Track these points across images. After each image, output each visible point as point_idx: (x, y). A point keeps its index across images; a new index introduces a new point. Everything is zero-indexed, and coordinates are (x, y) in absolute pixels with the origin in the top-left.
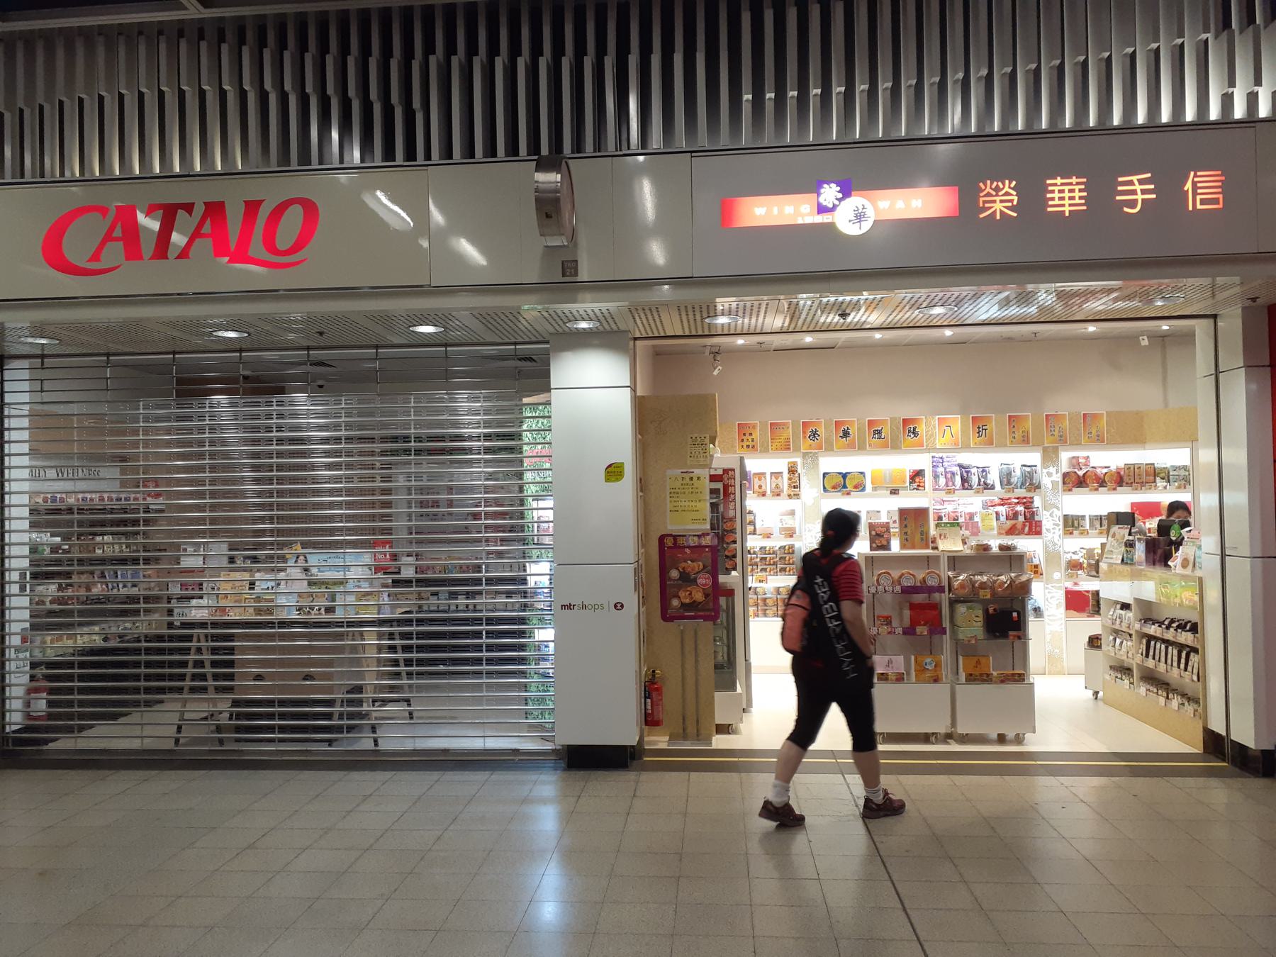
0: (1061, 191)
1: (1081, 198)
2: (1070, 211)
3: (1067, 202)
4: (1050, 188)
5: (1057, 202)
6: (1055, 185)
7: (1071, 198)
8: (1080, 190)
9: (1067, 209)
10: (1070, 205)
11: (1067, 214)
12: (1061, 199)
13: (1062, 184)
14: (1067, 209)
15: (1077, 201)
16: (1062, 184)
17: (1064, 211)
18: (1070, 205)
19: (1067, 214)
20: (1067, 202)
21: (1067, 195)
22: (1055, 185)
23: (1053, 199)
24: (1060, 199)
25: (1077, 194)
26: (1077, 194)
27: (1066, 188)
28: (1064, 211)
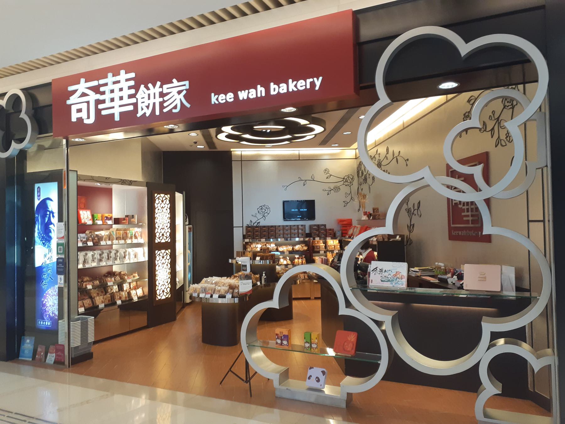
1: (130, 96)
2: (121, 114)
6: (106, 84)
8: (130, 88)
10: (120, 106)
11: (117, 118)
12: (112, 100)
15: (126, 101)
17: (113, 115)
18: (120, 106)
19: (117, 118)
20: (117, 102)
21: (116, 95)
22: (106, 84)
26: (126, 92)
27: (116, 87)
28: (113, 115)
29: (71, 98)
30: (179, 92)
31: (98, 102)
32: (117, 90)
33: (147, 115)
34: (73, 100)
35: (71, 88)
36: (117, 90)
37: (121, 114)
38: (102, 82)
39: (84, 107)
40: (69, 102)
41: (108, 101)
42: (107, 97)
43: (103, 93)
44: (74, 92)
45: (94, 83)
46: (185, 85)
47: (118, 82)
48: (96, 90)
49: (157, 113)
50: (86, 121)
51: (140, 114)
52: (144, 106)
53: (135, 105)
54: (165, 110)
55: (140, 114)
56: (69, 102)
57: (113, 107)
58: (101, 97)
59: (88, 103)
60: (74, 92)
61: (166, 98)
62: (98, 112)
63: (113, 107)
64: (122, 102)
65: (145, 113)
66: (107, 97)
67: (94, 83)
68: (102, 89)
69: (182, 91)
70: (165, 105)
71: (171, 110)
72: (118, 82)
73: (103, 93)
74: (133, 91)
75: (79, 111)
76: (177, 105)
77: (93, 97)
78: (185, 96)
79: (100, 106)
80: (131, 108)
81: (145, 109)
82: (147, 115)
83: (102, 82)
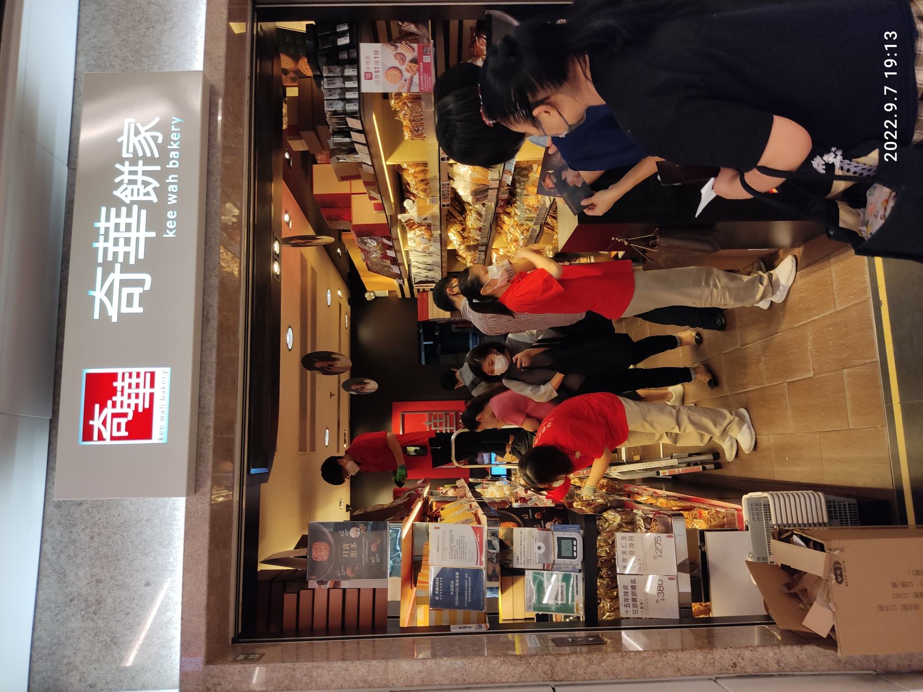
0: (116, 242)
1: (129, 214)
2: (148, 229)
3: (133, 235)
4: (110, 258)
5: (132, 249)
6: (106, 250)
7: (128, 227)
8: (118, 215)
9: (144, 234)
10: (138, 230)
11: (153, 234)
12: (127, 241)
13: (106, 240)
14: (144, 234)
15: (133, 220)
16: (106, 240)
18: (138, 230)
19: (153, 234)
20: (133, 235)
21: (122, 235)
22: (106, 250)
23: (127, 255)
24: (127, 241)
25: (123, 220)
26: (123, 220)
27: (112, 234)
29: (110, 315)
30: (137, 132)
31: (126, 268)
32: (117, 235)
33: (158, 185)
34: (113, 312)
35: (96, 316)
36: (117, 235)
37: (148, 229)
38: (100, 260)
39: (126, 291)
40: (114, 319)
41: (127, 249)
42: (121, 249)
43: (115, 254)
44: (102, 304)
45: (99, 270)
46: (129, 124)
47: (107, 229)
48: (108, 268)
49: (158, 168)
50: (147, 287)
51: (154, 198)
52: (143, 191)
53: (142, 205)
54: (157, 155)
55: (154, 198)
56: (114, 319)
57: (138, 239)
58: (121, 259)
59: (124, 283)
60: (102, 305)
61: (141, 154)
62: (140, 266)
63: (138, 239)
64: (134, 227)
65: (155, 189)
66: (121, 249)
67: (99, 270)
68: (110, 258)
69: (136, 127)
70: (149, 155)
71: (157, 145)
72: (107, 229)
73: (115, 254)
74: (124, 210)
75: (130, 297)
76: (152, 137)
77: (117, 276)
78: (143, 125)
79: (132, 261)
80: (144, 213)
81: (150, 188)
82: (158, 185)
83: (100, 260)
